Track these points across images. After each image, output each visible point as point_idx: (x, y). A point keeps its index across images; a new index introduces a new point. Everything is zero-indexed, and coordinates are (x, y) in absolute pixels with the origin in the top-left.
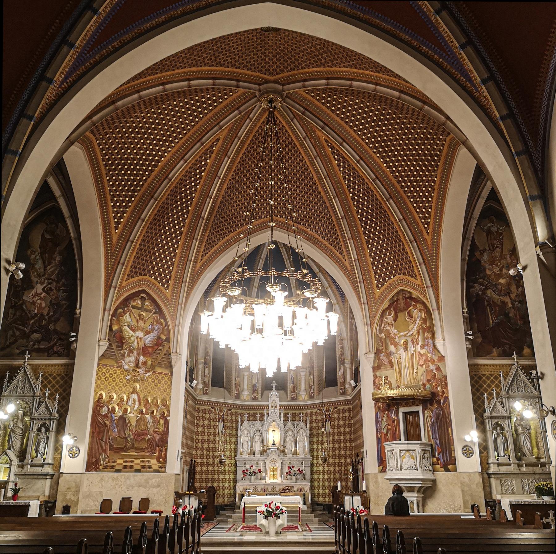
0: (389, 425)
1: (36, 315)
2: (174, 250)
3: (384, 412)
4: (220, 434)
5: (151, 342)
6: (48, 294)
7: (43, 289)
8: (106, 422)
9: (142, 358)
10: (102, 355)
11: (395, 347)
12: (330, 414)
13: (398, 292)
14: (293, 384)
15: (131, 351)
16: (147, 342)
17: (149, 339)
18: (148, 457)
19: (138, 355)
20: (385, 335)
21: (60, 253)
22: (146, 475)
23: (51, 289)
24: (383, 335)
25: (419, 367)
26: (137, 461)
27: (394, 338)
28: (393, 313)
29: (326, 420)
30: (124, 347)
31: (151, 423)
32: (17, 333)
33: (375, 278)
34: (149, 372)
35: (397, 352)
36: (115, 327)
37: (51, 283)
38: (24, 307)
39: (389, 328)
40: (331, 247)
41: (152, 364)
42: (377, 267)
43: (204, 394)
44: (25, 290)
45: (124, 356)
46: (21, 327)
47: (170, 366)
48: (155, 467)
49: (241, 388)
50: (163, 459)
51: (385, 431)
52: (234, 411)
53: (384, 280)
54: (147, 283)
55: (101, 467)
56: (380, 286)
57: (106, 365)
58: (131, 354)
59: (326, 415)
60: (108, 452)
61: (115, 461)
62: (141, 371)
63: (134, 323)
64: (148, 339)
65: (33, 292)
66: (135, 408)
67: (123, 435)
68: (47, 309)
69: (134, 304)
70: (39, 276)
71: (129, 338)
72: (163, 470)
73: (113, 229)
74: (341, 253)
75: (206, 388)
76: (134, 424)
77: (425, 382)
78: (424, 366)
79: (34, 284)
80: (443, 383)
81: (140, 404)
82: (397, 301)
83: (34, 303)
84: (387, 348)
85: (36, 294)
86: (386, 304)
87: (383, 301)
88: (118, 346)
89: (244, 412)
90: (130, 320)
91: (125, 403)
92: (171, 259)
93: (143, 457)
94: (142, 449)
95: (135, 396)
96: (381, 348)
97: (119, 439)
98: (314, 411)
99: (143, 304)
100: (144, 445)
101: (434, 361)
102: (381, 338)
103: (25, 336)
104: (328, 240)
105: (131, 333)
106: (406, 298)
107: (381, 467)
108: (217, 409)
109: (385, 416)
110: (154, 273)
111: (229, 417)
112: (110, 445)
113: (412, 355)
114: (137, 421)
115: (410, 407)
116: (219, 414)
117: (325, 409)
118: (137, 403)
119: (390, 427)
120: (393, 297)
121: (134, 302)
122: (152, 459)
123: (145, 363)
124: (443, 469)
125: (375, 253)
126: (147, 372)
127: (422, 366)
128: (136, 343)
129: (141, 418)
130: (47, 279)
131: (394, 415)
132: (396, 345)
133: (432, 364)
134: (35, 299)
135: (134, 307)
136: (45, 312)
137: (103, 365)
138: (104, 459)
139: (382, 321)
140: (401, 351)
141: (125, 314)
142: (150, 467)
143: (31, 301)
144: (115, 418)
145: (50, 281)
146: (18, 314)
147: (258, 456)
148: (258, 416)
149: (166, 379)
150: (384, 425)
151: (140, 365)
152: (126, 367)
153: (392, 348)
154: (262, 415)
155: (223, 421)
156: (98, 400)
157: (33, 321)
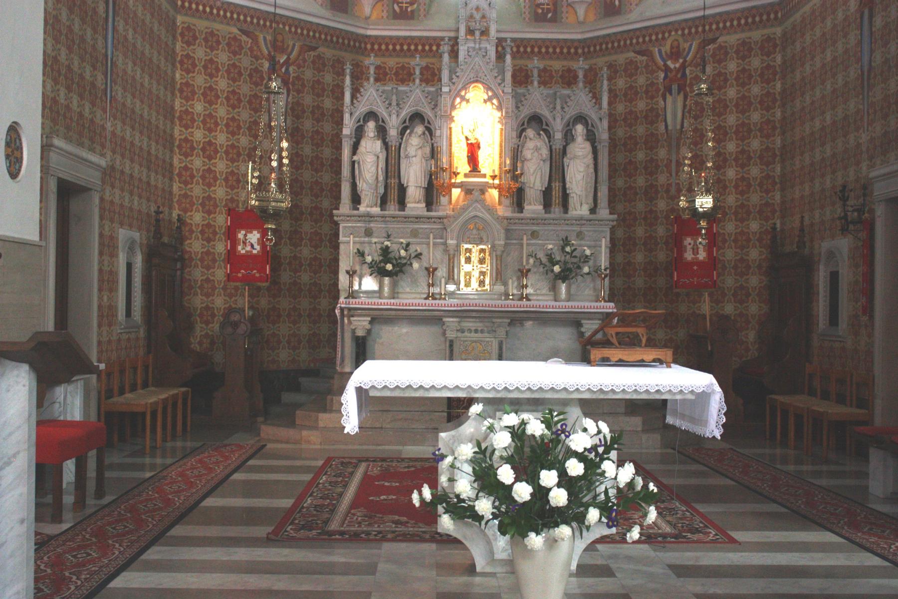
12: (683, 67)
52: (328, 53)
59: (667, 69)
98: (621, 58)
111: (308, 74)
117: (667, 48)
147: (415, 203)
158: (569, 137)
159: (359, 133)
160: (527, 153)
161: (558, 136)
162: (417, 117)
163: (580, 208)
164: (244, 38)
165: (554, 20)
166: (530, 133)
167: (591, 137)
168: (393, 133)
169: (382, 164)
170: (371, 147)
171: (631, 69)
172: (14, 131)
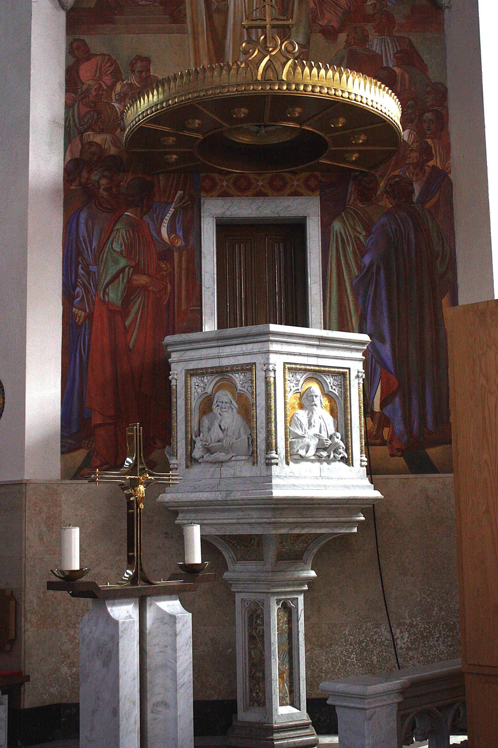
0: (137, 269)
51: (114, 296)
78: (342, 37)
80: (428, 115)
101: (391, 21)
107: (80, 456)
109: (121, 231)
115: (260, 201)
119: (142, 280)
124: (400, 461)
131: (171, 230)
133: (380, 31)
150: (113, 270)
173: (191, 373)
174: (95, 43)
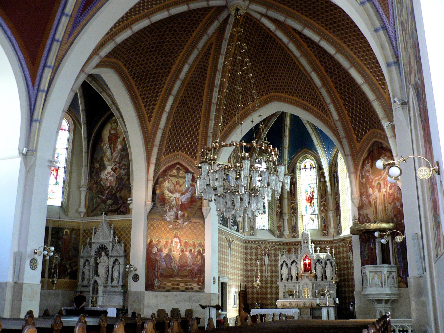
1: (109, 187)
2: (197, 130)
3: (366, 243)
4: (266, 265)
5: (186, 200)
6: (115, 172)
7: (112, 169)
8: (157, 258)
9: (180, 212)
10: (150, 212)
11: (373, 190)
13: (373, 143)
14: (324, 223)
15: (171, 208)
16: (183, 200)
17: (185, 198)
18: (190, 281)
19: (177, 210)
20: (365, 180)
21: (120, 143)
22: (189, 294)
23: (116, 169)
24: (364, 180)
25: (389, 205)
26: (182, 285)
27: (372, 182)
28: (370, 161)
29: (349, 251)
30: (166, 205)
31: (191, 258)
32: (99, 200)
33: (355, 133)
34: (186, 222)
35: (374, 193)
36: (158, 192)
37: (116, 165)
38: (102, 183)
39: (367, 174)
40: (320, 112)
41: (188, 216)
42: (355, 124)
43: (251, 235)
44: (102, 171)
45: (166, 211)
46: (101, 196)
47: (202, 217)
48: (195, 289)
49: (282, 229)
50: (202, 283)
51: (367, 258)
52: (277, 247)
53: (362, 134)
54: (181, 157)
55: (156, 288)
56: (359, 140)
57: (154, 219)
58: (171, 210)
59: (349, 247)
60: (160, 279)
61: (165, 284)
62: (180, 222)
63: (172, 187)
64: (184, 198)
65: (106, 172)
66: (178, 248)
67: (170, 267)
68: (115, 182)
69: (171, 173)
70: (109, 160)
71: (169, 198)
72: (203, 291)
73: (148, 122)
74: (327, 116)
75: (252, 231)
76: (178, 259)
77: (393, 217)
78: (392, 204)
79: (106, 166)
81: (181, 245)
82: (372, 151)
83: (107, 179)
84: (367, 191)
85: (108, 173)
86: (365, 155)
87: (363, 153)
88: (161, 205)
89: (292, 247)
90: (169, 186)
91: (169, 244)
92: (196, 137)
93: (187, 281)
94: (185, 276)
95: (177, 240)
96: (363, 191)
97: (167, 269)
98: (341, 244)
99: (178, 173)
100: (186, 273)
102: (363, 183)
103: (104, 202)
104: (316, 106)
105: (171, 195)
106: (379, 148)
108: (263, 246)
109: (367, 246)
110: (185, 149)
111: (273, 252)
112: (161, 274)
113: (384, 195)
114: (180, 257)
116: (264, 250)
117: (349, 242)
118: (179, 245)
120: (370, 148)
121: (171, 172)
122: (193, 283)
123: (183, 216)
125: (352, 113)
126: (184, 222)
127: (390, 203)
128: (174, 202)
129: (182, 255)
130: (114, 162)
132: (373, 187)
134: (107, 177)
135: (171, 176)
136: (114, 185)
137: (151, 219)
138: (157, 283)
139: (363, 169)
140: (377, 192)
141: (165, 181)
142: (192, 289)
143: (105, 178)
144: (163, 255)
145: (116, 163)
146: (99, 187)
148: (293, 250)
149: (200, 226)
151: (179, 217)
152: (168, 219)
153: (370, 191)
154: (296, 250)
155: (268, 255)
156: (150, 243)
157: (107, 192)
158: (326, 264)
159: (282, 265)
160: (317, 268)
161: (324, 264)
162: (294, 262)
163: (329, 279)
164: (258, 247)
165: (327, 235)
166: (317, 263)
167: (331, 264)
168: (289, 265)
169: (287, 272)
170: (285, 269)
171: (343, 247)
172: (214, 278)
173: (370, 272)
174: (361, 212)
